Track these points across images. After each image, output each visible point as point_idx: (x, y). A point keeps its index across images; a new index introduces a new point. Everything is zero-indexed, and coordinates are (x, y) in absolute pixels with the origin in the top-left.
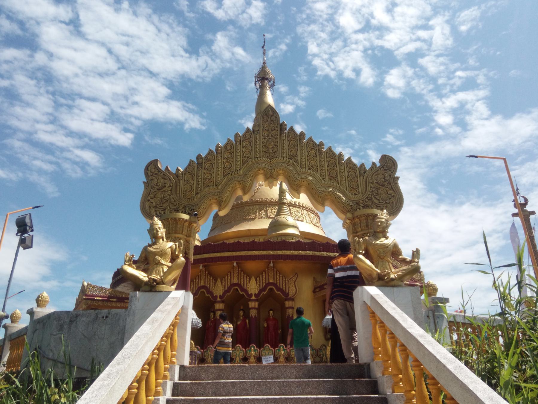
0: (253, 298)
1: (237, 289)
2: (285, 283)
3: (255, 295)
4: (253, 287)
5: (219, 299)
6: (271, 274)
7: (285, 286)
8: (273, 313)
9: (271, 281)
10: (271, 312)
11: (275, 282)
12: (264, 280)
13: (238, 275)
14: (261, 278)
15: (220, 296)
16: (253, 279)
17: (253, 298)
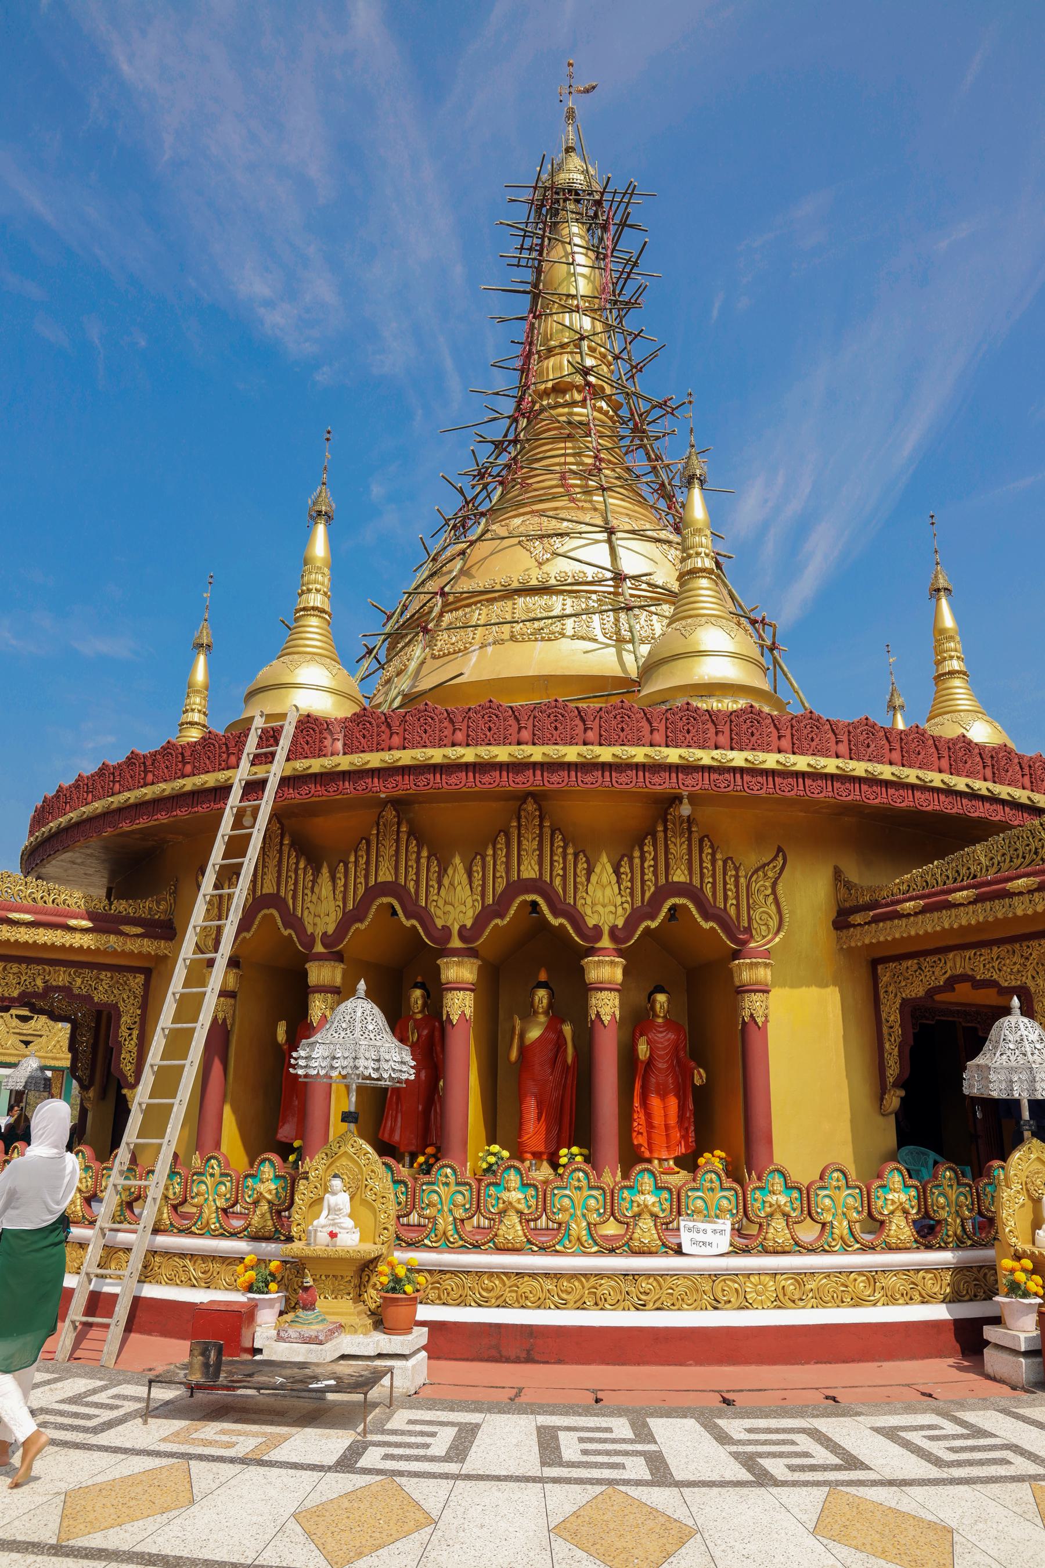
0: (606, 942)
1: (534, 904)
2: (737, 886)
3: (613, 931)
4: (604, 900)
5: (456, 943)
6: (679, 848)
7: (737, 898)
8: (669, 1001)
9: (679, 876)
10: (661, 998)
11: (696, 882)
12: (649, 876)
13: (540, 848)
14: (637, 861)
15: (463, 927)
16: (604, 870)
17: (606, 942)
